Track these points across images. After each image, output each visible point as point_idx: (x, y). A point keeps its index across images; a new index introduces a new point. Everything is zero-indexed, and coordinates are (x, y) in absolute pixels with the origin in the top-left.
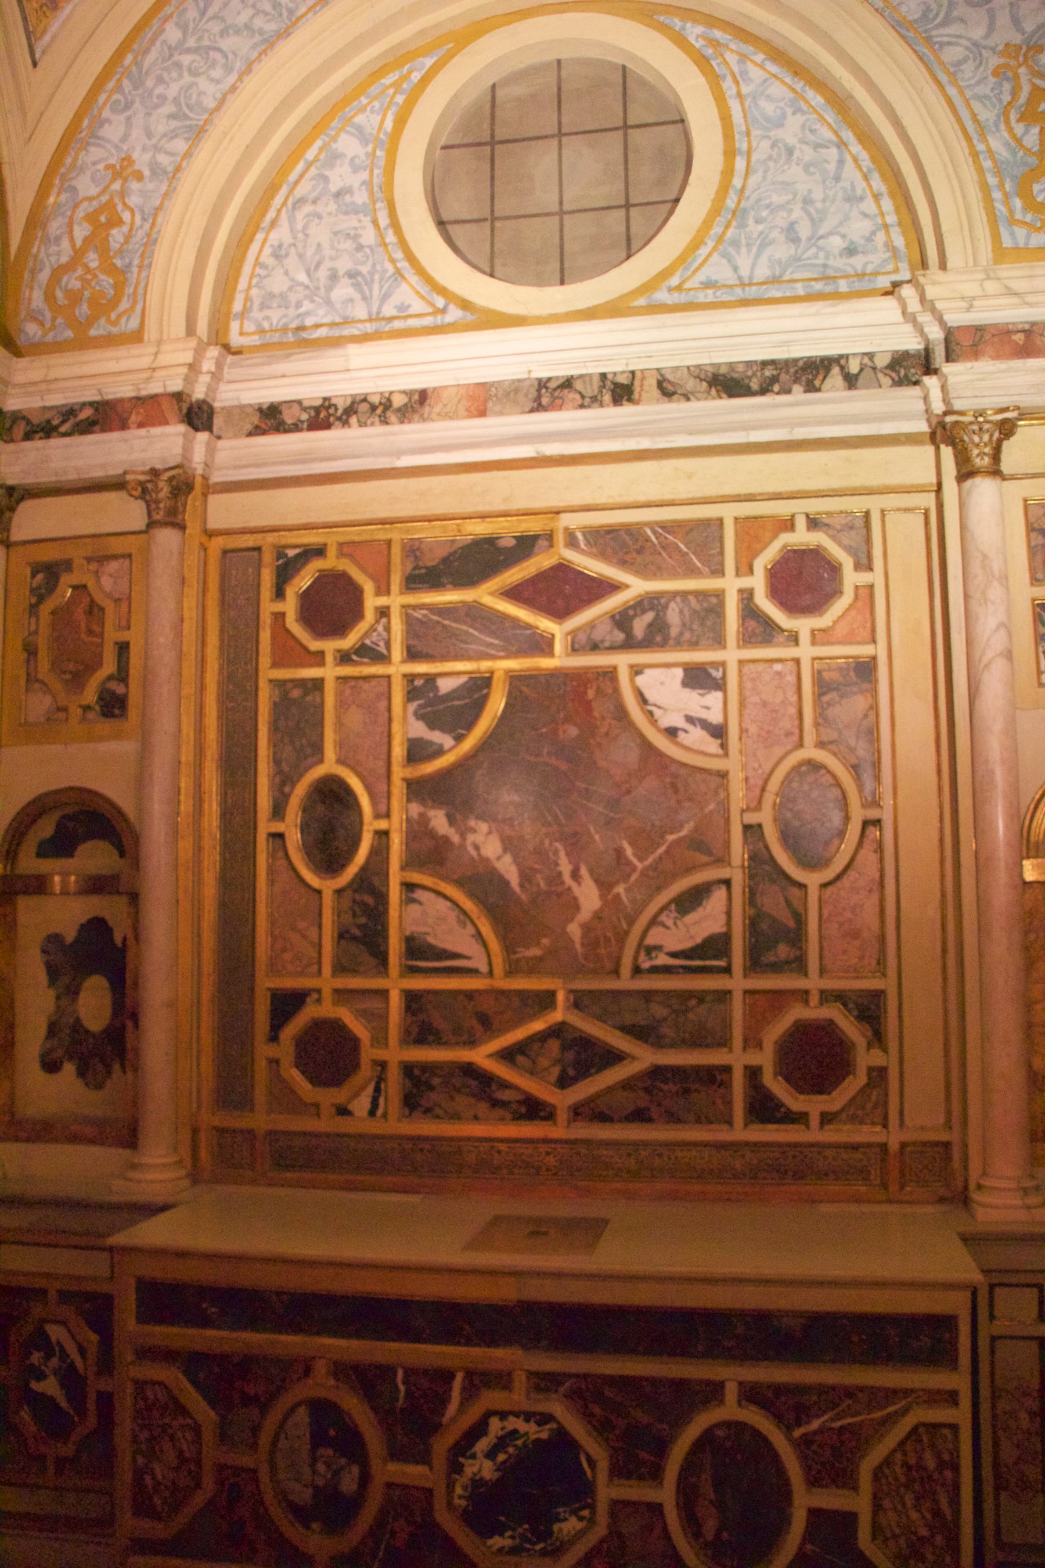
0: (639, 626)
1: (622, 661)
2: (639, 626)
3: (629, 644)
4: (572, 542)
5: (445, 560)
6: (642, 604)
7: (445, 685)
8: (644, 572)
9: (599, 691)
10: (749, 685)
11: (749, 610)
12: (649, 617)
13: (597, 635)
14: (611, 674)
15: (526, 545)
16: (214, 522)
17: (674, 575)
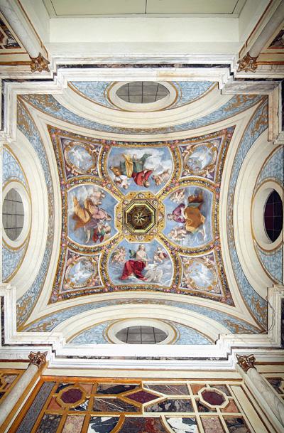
0: (167, 407)
1: (163, 414)
2: (167, 407)
3: (164, 410)
4: (145, 386)
5: (109, 389)
6: (167, 401)
7: (104, 419)
8: (167, 393)
9: (155, 423)
10: (204, 423)
11: (199, 404)
12: (170, 404)
13: (154, 408)
14: (160, 419)
15: (132, 387)
16: (44, 374)
17: (175, 394)
